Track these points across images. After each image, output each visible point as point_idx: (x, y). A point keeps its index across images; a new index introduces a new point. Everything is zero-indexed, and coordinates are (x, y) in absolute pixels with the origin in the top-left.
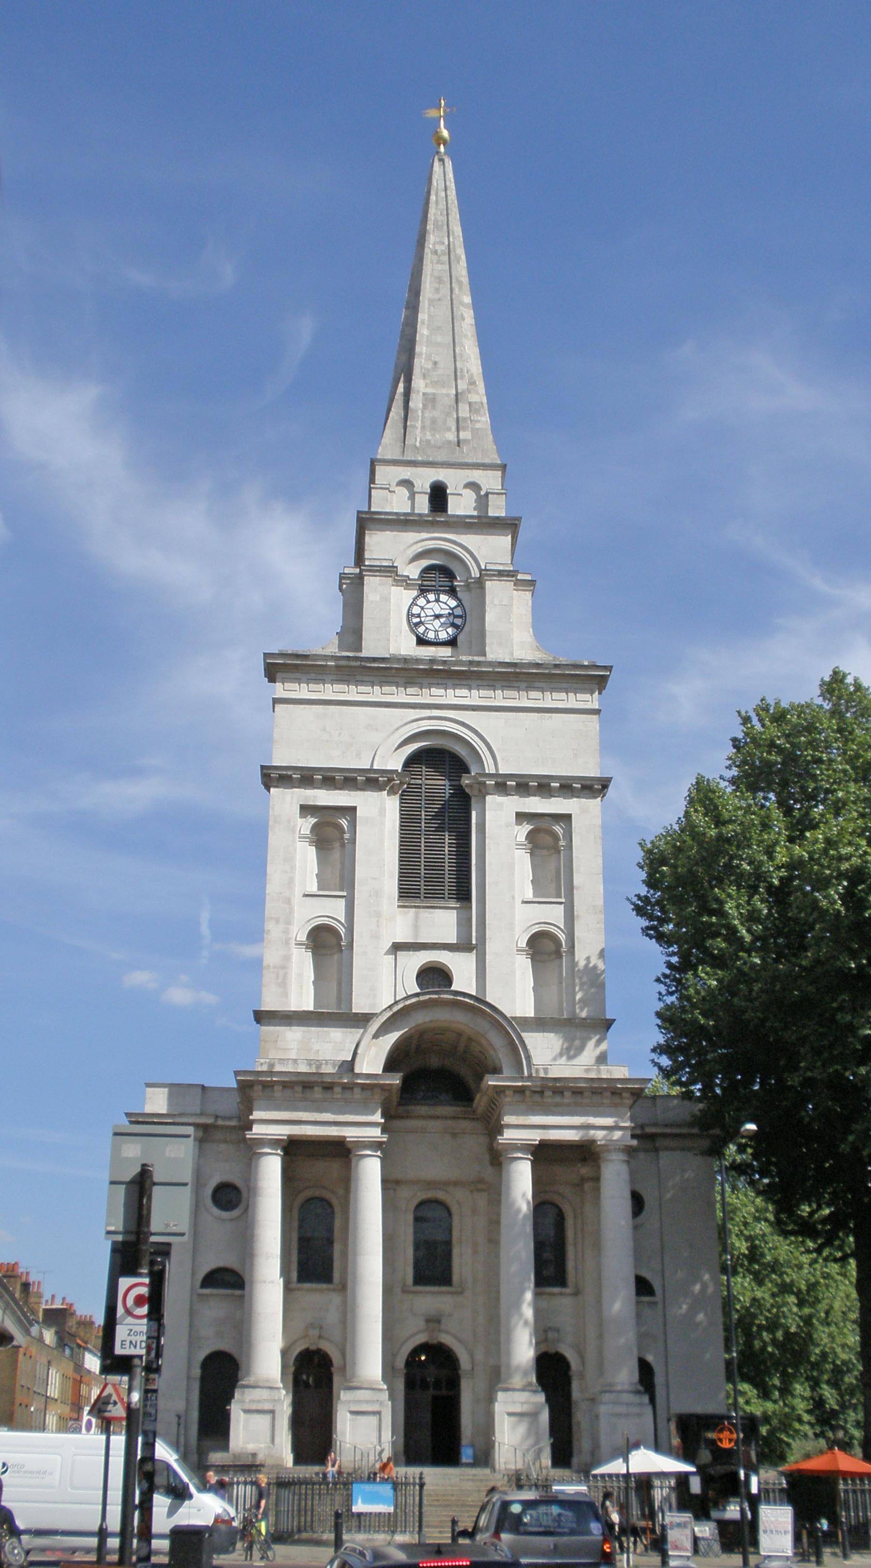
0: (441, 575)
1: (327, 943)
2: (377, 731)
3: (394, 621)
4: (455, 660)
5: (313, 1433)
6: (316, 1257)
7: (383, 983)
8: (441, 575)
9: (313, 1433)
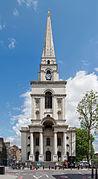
0: (49, 72)
1: (38, 113)
2: (41, 90)
3: (43, 77)
4: (49, 82)
5: (37, 159)
6: (37, 143)
7: (43, 116)
8: (49, 72)
9: (37, 159)
